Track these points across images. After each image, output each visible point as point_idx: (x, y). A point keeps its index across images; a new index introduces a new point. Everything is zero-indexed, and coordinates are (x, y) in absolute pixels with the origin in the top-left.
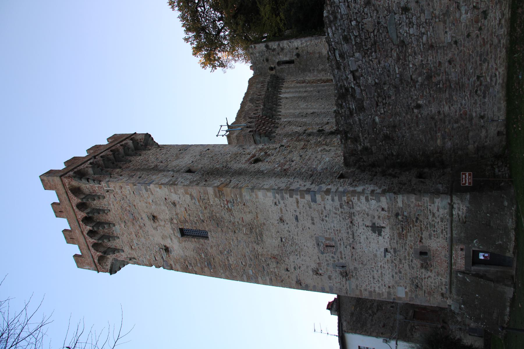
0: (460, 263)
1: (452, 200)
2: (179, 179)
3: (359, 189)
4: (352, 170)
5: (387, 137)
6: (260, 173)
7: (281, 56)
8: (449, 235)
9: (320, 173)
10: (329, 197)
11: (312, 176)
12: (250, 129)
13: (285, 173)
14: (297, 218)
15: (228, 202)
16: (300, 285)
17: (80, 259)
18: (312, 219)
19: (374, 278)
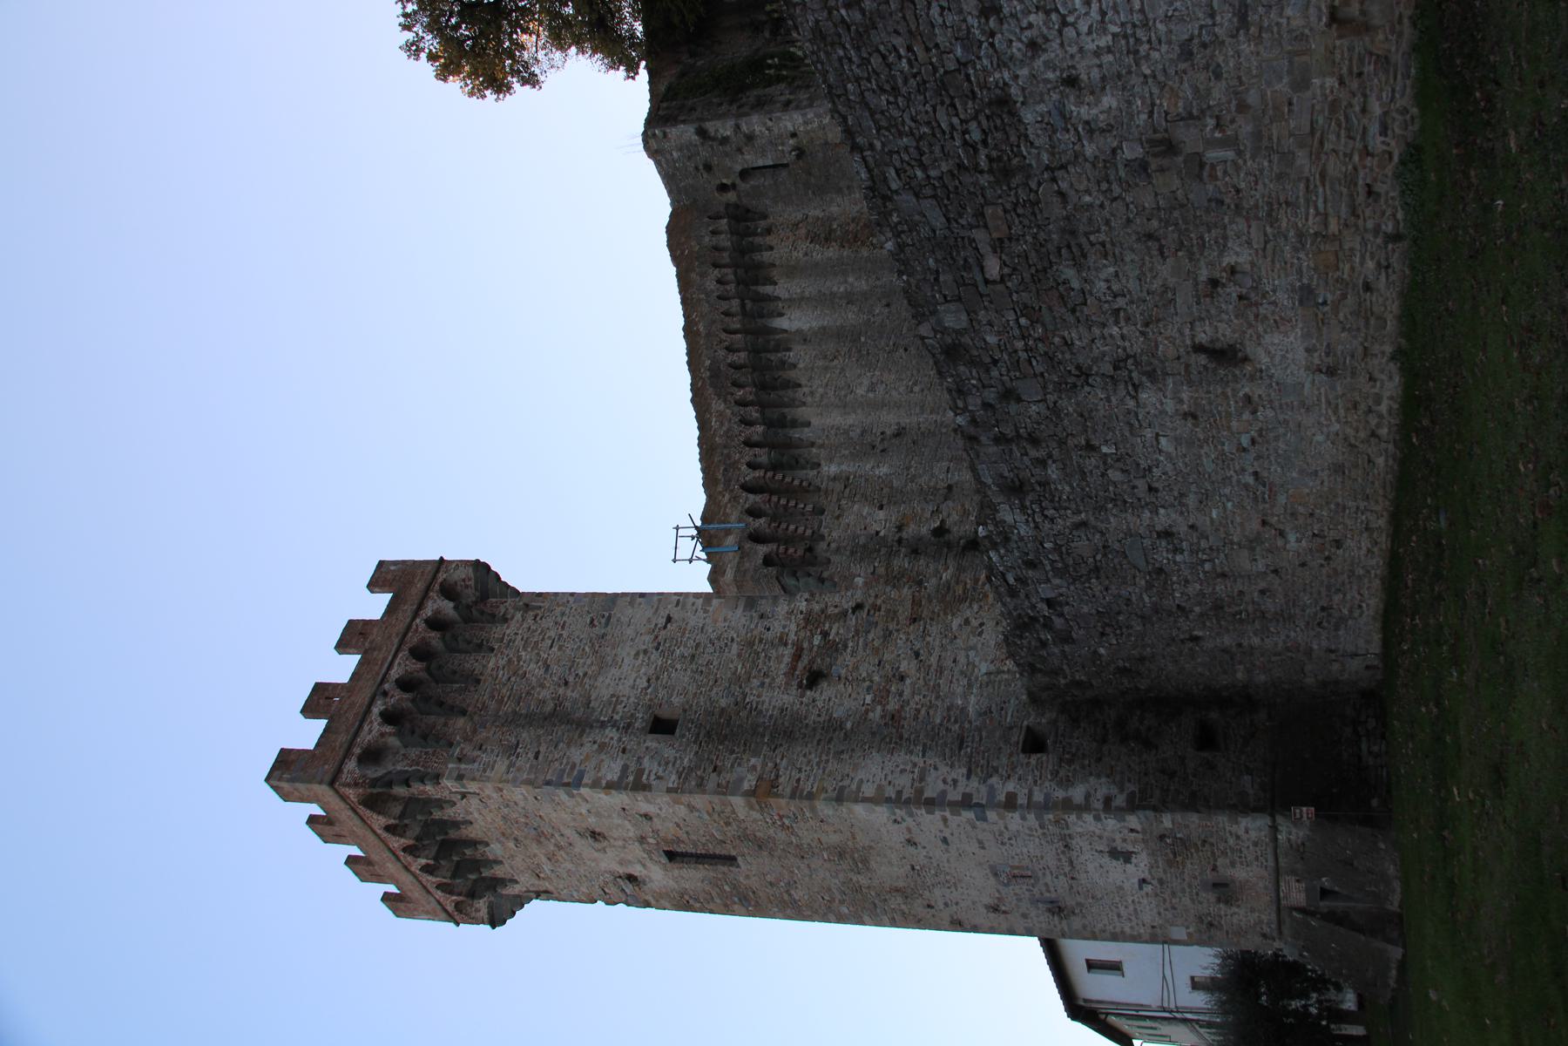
0: (1296, 893)
1: (1274, 821)
2: (646, 762)
3: (1077, 793)
4: (1048, 715)
5: (1123, 671)
6: (835, 735)
7: (747, 157)
8: (1271, 863)
9: (979, 729)
10: (1017, 815)
11: (958, 740)
12: (763, 550)
13: (892, 732)
14: (945, 841)
15: (781, 817)
16: (958, 925)
17: (402, 906)
18: (980, 842)
19: (1119, 916)
